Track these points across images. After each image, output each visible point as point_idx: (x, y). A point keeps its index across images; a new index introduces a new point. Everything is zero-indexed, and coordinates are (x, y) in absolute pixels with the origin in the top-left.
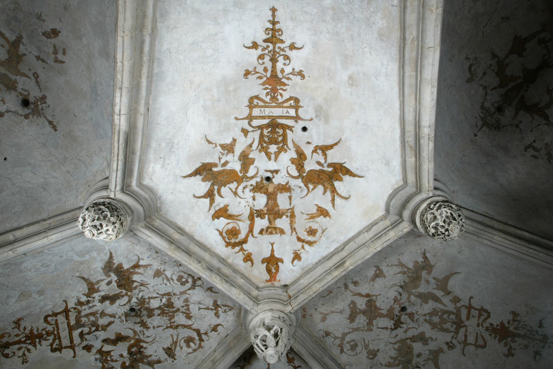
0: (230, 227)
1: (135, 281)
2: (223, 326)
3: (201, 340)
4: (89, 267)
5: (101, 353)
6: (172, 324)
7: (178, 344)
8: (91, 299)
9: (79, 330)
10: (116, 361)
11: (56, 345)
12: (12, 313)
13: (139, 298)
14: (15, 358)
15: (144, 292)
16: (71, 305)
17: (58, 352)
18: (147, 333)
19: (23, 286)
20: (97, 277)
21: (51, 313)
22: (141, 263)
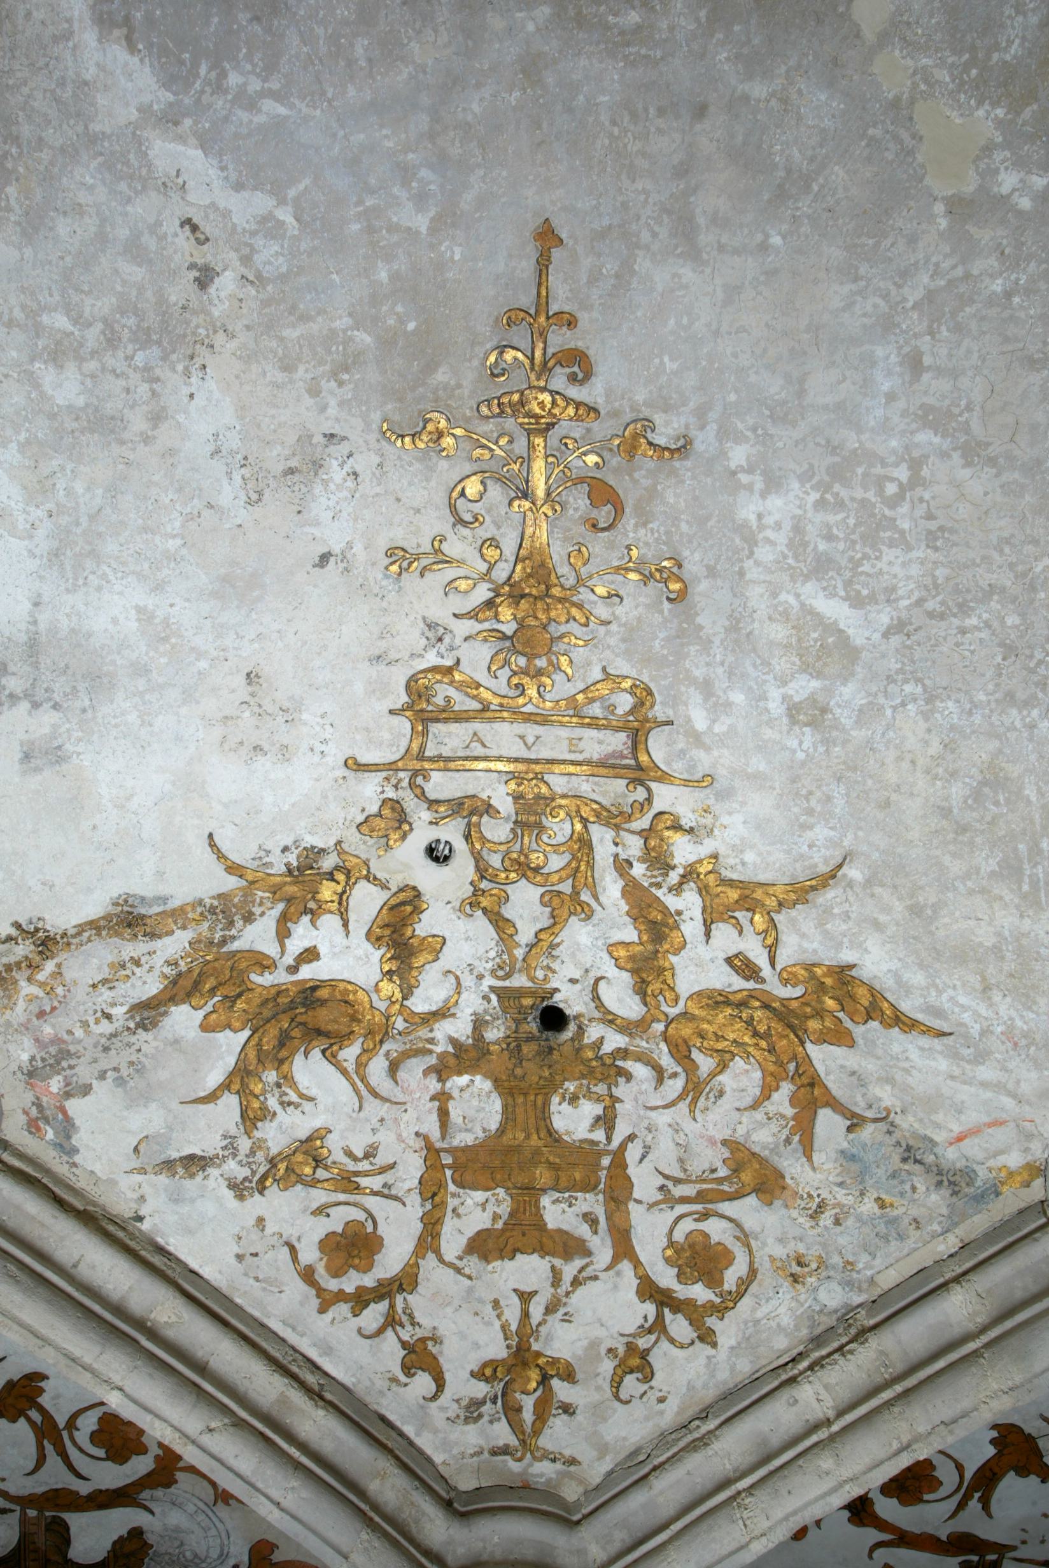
0: (947, 1475)
1: (723, 1067)
2: (434, 1398)
3: (360, 1300)
4: (878, 926)
5: (341, 877)
6: (448, 1173)
7: (342, 1197)
8: (674, 877)
9: (504, 804)
10: (283, 934)
11: (448, 699)
12: (741, 573)
13: (619, 1063)
14: (436, 522)
15: (649, 1086)
16: (665, 797)
17: (404, 698)
18: (414, 1072)
19: (901, 671)
20: (803, 936)
21: (659, 712)
22: (828, 1123)
